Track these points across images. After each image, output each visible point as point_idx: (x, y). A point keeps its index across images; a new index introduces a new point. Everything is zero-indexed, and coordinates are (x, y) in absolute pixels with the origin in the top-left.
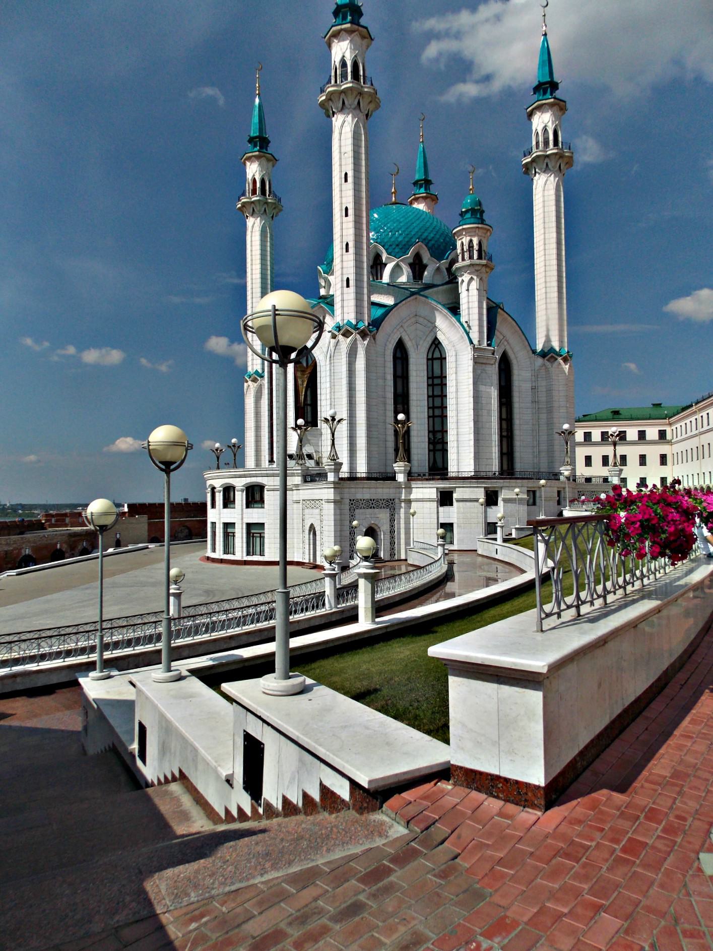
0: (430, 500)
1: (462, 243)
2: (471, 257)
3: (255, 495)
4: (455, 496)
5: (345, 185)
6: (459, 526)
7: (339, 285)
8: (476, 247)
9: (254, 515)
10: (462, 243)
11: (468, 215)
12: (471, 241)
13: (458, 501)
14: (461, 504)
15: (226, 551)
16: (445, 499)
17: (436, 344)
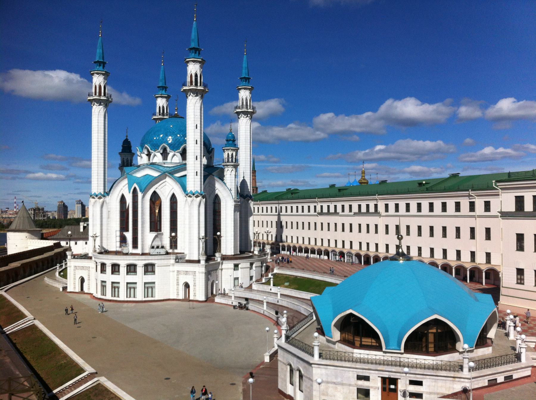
0: (231, 269)
1: (228, 154)
2: (232, 162)
3: (149, 268)
4: (240, 266)
5: (196, 130)
6: (241, 278)
7: (193, 174)
8: (234, 157)
9: (149, 278)
10: (228, 154)
11: (231, 142)
12: (232, 154)
13: (241, 268)
14: (242, 270)
15: (113, 295)
16: (236, 266)
17: (217, 196)
